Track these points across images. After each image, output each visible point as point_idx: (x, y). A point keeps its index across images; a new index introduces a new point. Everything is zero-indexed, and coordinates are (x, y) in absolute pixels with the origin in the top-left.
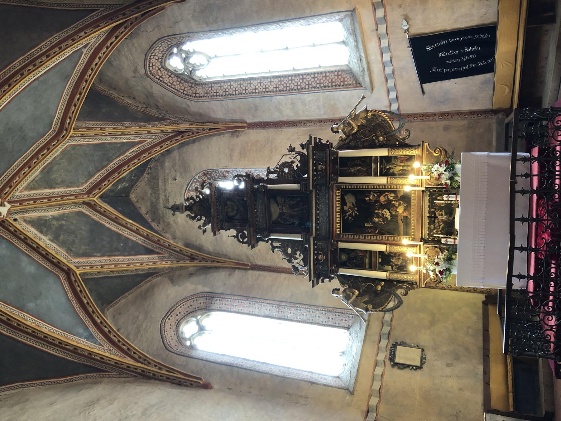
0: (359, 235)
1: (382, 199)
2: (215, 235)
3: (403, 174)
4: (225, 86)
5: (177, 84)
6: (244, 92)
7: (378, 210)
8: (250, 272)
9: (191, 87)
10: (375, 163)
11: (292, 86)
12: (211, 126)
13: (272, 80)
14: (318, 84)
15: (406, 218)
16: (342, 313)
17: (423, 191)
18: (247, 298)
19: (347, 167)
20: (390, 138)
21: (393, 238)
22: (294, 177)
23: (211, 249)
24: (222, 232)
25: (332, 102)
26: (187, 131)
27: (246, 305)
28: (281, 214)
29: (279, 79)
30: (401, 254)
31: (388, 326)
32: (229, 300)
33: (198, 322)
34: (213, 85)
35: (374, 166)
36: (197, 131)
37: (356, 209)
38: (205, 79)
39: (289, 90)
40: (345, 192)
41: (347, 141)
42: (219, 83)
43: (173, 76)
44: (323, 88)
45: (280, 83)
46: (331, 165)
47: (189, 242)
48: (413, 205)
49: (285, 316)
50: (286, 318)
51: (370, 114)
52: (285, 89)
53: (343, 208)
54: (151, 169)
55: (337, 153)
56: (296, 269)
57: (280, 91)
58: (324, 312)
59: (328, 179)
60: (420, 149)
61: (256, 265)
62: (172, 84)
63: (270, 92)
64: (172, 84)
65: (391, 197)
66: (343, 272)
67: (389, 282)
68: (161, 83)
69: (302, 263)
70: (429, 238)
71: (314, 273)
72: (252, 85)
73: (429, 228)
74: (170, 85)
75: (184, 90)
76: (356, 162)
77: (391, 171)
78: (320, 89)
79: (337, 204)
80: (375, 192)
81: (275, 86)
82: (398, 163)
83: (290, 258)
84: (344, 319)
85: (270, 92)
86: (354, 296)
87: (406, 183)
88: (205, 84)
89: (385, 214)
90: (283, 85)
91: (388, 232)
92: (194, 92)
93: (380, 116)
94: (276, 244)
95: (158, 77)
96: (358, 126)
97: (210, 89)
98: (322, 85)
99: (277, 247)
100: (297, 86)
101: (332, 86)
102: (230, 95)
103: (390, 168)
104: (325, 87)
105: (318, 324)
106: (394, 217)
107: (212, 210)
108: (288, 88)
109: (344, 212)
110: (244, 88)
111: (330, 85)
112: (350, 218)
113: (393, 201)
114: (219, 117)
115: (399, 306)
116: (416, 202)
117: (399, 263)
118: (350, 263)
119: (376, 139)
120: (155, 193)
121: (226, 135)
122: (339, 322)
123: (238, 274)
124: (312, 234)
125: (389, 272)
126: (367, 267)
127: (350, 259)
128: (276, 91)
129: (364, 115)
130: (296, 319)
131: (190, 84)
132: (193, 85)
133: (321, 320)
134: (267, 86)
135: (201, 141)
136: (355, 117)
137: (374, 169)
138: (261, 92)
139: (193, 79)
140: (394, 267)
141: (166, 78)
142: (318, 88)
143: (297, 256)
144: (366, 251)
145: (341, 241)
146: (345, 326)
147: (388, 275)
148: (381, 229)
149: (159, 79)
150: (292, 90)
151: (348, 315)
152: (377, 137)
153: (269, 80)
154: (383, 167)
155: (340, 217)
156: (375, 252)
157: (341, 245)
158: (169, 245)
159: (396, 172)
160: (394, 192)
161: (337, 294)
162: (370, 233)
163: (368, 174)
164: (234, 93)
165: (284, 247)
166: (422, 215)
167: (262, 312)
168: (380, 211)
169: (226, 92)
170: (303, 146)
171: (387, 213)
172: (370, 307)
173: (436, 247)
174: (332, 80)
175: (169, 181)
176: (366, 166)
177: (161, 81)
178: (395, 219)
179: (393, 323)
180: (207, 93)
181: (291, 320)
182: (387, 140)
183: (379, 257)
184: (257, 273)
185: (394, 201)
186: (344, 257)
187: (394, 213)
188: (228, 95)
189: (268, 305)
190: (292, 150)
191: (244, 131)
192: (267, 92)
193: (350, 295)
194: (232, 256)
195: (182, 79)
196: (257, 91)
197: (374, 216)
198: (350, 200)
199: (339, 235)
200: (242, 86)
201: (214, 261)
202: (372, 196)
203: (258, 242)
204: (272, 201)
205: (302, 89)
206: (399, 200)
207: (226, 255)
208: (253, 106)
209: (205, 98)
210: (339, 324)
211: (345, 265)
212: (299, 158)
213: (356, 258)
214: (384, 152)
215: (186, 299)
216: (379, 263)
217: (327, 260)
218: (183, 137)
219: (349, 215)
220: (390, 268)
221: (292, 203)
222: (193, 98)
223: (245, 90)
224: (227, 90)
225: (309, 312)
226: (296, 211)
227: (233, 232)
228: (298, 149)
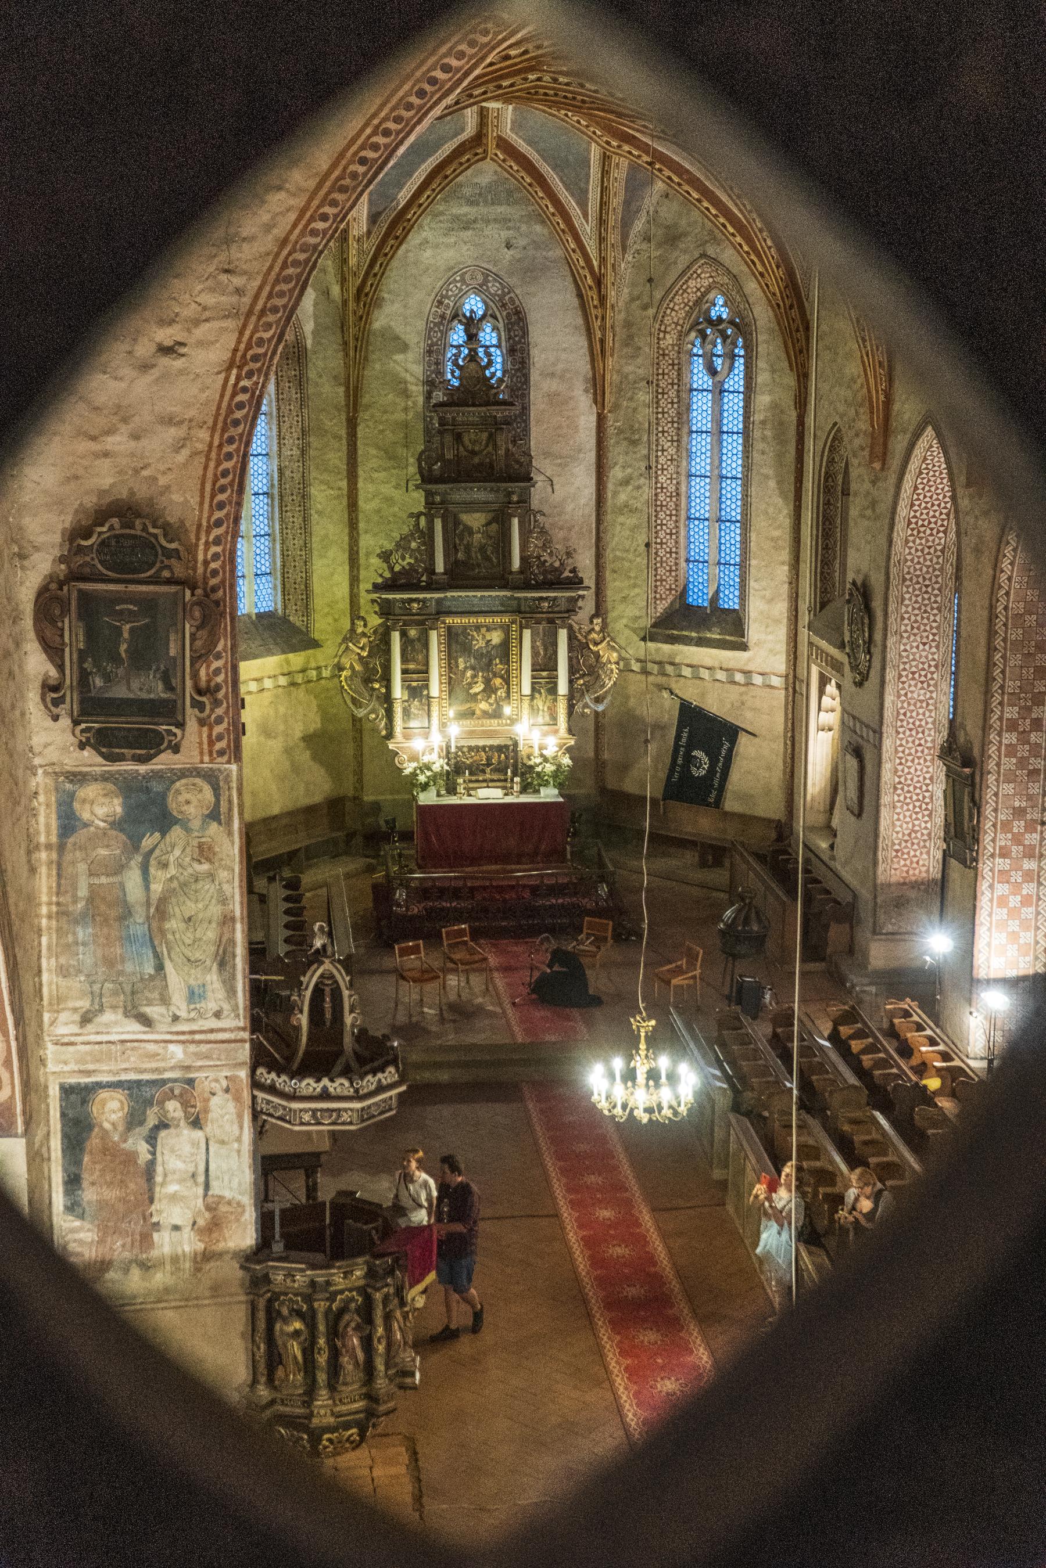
1: (498, 681)
15: (473, 713)
28: (469, 530)
65: (501, 693)
66: (396, 637)
77: (537, 695)
80: (508, 671)
83: (402, 544)
94: (423, 521)
109: (478, 628)
144: (427, 664)
156: (427, 680)
157: (433, 635)
170: (574, 571)
171: (478, 688)
186: (413, 633)
204: (490, 515)
211: (404, 634)
212: (557, 564)
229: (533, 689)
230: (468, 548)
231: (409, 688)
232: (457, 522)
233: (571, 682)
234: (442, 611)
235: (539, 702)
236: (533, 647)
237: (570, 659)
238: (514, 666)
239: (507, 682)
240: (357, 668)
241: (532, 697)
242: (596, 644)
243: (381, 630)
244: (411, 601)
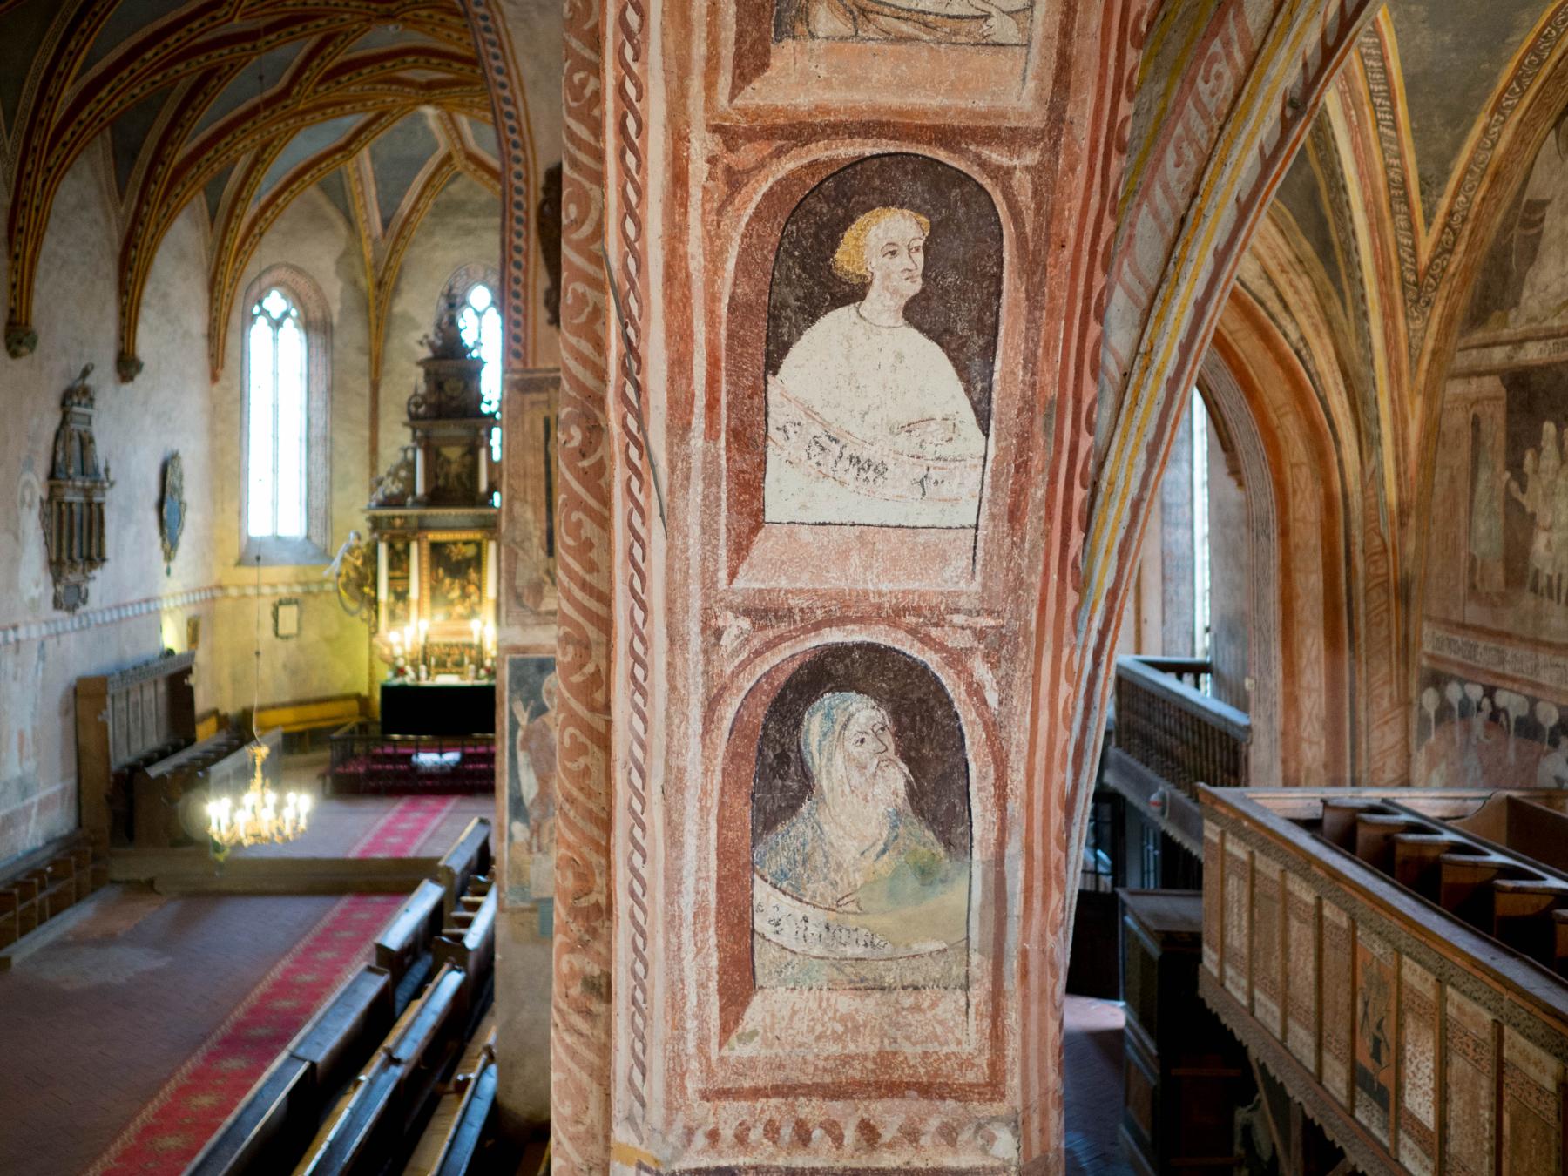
1: (472, 589)
27: (321, 387)
28: (449, 462)
33: (286, 314)
56: (380, 482)
65: (475, 598)
79: (464, 536)
80: (480, 580)
83: (394, 474)
106: (451, 603)
109: (455, 543)
123: (363, 361)
157: (414, 547)
171: (456, 594)
186: (399, 546)
198: (470, 551)
204: (465, 449)
211: (391, 547)
215: (318, 290)
221: (464, 477)
227: (423, 389)
230: (447, 476)
232: (438, 454)
234: (423, 527)
240: (353, 574)
244: (394, 517)
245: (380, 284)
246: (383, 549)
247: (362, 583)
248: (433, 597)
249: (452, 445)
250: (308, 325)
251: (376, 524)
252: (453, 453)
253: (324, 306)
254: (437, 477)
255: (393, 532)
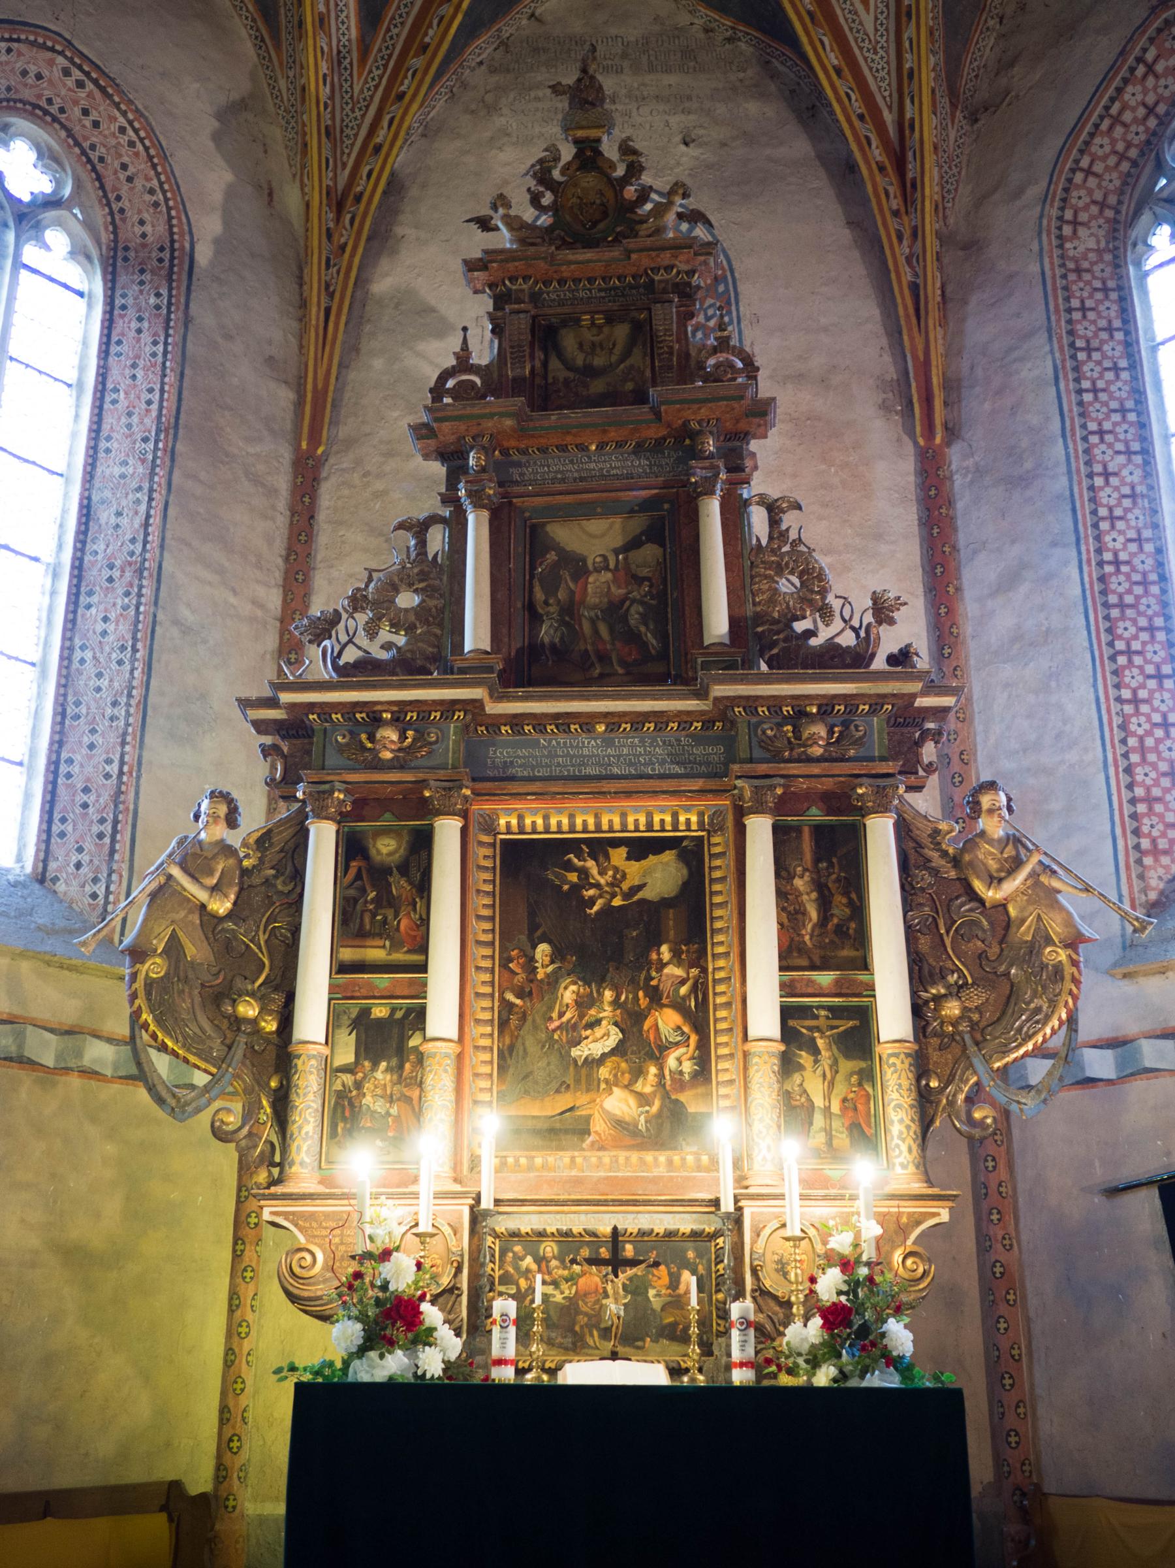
0: (492, 919)
1: (667, 1021)
2: (471, 266)
3: (796, 1110)
4: (1113, 349)
5: (1113, 142)
6: (1092, 426)
7: (615, 1003)
8: (286, 454)
9: (1103, 205)
10: (837, 982)
11: (1126, 629)
12: (933, 292)
13: (1149, 547)
14: (1141, 739)
15: (582, 1130)
16: (112, 851)
17: (716, 1203)
18: (171, 428)
19: (817, 860)
20: (956, 1049)
21: (486, 1069)
22: (758, 618)
23: (383, 284)
24: (485, 303)
25: (1055, 806)
26: (909, 190)
27: (134, 420)
28: (578, 566)
29: (1153, 577)
30: (415, 1109)
31: (58, 1058)
32: (161, 348)
34: (1114, 296)
35: (825, 978)
36: (907, 234)
37: (617, 902)
38: (1138, 264)
39: (1107, 618)
40: (692, 854)
41: (935, 855)
42: (1125, 322)
43: (1152, 123)
44: (1123, 764)
45: (1136, 577)
46: (827, 784)
47: (414, 192)
48: (642, 1162)
49: (90, 593)
50: (83, 600)
51: (1063, 956)
52: (1113, 599)
53: (616, 843)
54: (729, 40)
55: (882, 808)
57: (1102, 579)
58: (114, 769)
59: (763, 768)
60: (918, 1187)
61: (316, 479)
62: (1117, 120)
63: (1098, 538)
64: (1117, 120)
65: (679, 1060)
67: (281, 1054)
68: (1124, 72)
69: (350, 655)
70: (497, 1236)
71: (311, 707)
72: (1121, 459)
73: (542, 1234)
74: (1114, 110)
75: (1088, 172)
76: (839, 899)
77: (805, 1058)
78: (1120, 750)
80: (700, 988)
81: (1123, 556)
82: (841, 1089)
83: (372, 601)
84: (85, 858)
85: (1098, 538)
86: (202, 896)
87: (757, 1126)
88: (1118, 265)
89: (599, 1032)
90: (1129, 592)
91: (511, 1048)
92: (1083, 217)
93: (1053, 1005)
94: (437, 540)
95: (1150, 56)
96: (1002, 906)
97: (1097, 284)
98: (1135, 758)
99: (422, 543)
100: (1129, 652)
101: (1133, 801)
102: (1076, 369)
103: (815, 1051)
104: (1129, 770)
105: (58, 742)
107: (588, 255)
108: (1115, 613)
109: (599, 847)
110: (1107, 426)
111: (1139, 792)
112: (573, 877)
113: (661, 1069)
114: (970, 324)
115: (160, 1101)
116: (661, 1171)
117: (368, 1100)
118: (359, 876)
119: (948, 987)
120: (624, 56)
121: (887, 358)
122: (71, 839)
124: (498, 698)
125: (326, 1051)
126: (348, 954)
127: (379, 874)
128: (1100, 564)
129: (1056, 928)
130: (78, 642)
131: (1112, 200)
132: (1109, 213)
133: (77, 758)
134: (1120, 525)
135: (856, 254)
136: (1041, 893)
137: (810, 982)
138: (1093, 500)
139: (1137, 213)
140: (348, 1079)
141: (1145, 92)
142: (1124, 741)
143: (385, 635)
144: (423, 948)
145: (464, 831)
146: (53, 865)
147: (313, 1050)
148: (524, 1018)
149: (1139, 60)
150: (1109, 631)
151: (103, 876)
152: (957, 991)
153: (1147, 533)
154: (821, 1022)
155: (572, 830)
156: (421, 990)
157: (447, 833)
158: (401, 97)
159: (797, 1078)
160: (703, 1071)
161: (215, 818)
162: (504, 965)
163: (790, 955)
164: (1086, 384)
165: (423, 576)
166: (604, 1203)
167: (107, 494)
168: (607, 1012)
169: (1089, 350)
171: (601, 1041)
172: (155, 967)
173: (459, 1270)
174: (1158, 800)
175: (683, 117)
176: (827, 937)
177: (1132, 70)
178: (578, 1081)
179: (75, 1081)
180: (1078, 271)
181: (71, 623)
182: (941, 1035)
183: (393, 1010)
184: (282, 482)
185: (661, 1076)
186: (386, 848)
187: (604, 1072)
188: (1074, 357)
189: (138, 521)
190: (883, 610)
191: (912, 434)
192: (1095, 526)
193: (211, 873)
194: (352, 375)
195: (1135, 164)
196: (1099, 481)
197: (587, 983)
198: (660, 877)
199: (489, 827)
200: (1116, 417)
201: (331, 295)
202: (679, 972)
203: (443, 456)
204: (638, 524)
205: (1115, 673)
206: (666, 1096)
207: (357, 350)
208: (1028, 465)
209: (1057, 261)
210: (62, 835)
211: (351, 849)
212: (848, 639)
213: (386, 900)
214: (893, 1018)
216: (366, 1012)
217: (378, 765)
218: (882, 169)
219: (584, 873)
220: (346, 1055)
221: (635, 614)
222: (1054, 212)
223: (1101, 433)
224: (1096, 356)
225: (115, 704)
226: (596, 632)
227: (483, 352)
228: (890, 641)
229: (788, 1035)
230: (569, 611)
231: (362, 1023)
233: (917, 1010)
235: (813, 1083)
236: (781, 894)
237: (911, 934)
238: (719, 967)
239: (698, 1021)
241: (788, 1066)
242: (994, 880)
243: (279, 840)
244: (373, 717)
245: (339, 202)
246: (323, 839)
247: (217, 986)
248: (506, 1057)
249: (587, 511)
250: (116, 258)
251: (295, 741)
252: (595, 538)
253: (172, 203)
254: (534, 616)
255: (357, 779)
